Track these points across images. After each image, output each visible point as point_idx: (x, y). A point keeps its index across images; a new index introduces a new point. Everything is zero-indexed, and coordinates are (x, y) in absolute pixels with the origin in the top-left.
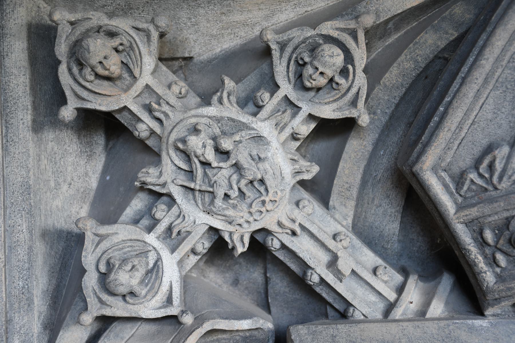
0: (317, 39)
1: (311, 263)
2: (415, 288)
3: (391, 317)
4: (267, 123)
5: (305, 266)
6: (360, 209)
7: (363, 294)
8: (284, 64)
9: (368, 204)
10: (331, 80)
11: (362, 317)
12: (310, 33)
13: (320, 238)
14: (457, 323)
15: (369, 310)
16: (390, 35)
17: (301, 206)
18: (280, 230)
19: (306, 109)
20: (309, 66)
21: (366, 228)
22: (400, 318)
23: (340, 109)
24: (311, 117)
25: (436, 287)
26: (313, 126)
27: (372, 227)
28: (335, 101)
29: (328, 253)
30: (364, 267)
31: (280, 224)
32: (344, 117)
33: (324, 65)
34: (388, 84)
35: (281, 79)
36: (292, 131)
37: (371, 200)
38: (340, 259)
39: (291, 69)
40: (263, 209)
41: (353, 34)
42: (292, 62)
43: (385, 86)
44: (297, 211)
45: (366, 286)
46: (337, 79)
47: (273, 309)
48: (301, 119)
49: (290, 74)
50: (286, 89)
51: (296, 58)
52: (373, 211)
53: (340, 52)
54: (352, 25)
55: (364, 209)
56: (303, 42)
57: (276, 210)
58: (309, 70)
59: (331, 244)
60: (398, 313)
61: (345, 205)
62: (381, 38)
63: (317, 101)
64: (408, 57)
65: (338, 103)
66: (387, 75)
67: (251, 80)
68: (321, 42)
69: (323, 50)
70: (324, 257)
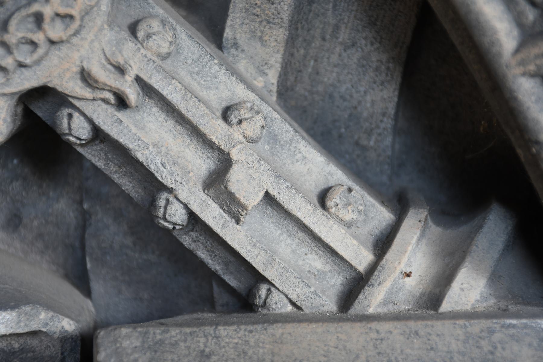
1: (165, 176)
2: (419, 240)
3: (356, 308)
5: (154, 186)
6: (302, 51)
7: (294, 252)
9: (324, 39)
11: (290, 308)
13: (189, 115)
14: (514, 326)
15: (306, 290)
17: (141, 34)
18: (87, 93)
21: (317, 98)
22: (380, 310)
25: (470, 239)
27: (331, 96)
29: (208, 153)
30: (296, 187)
31: (86, 77)
37: (330, 30)
38: (235, 167)
40: (39, 37)
44: (130, 45)
45: (301, 235)
47: (96, 286)
52: (334, 58)
55: (312, 52)
57: (75, 40)
59: (216, 129)
60: (373, 300)
61: (261, 38)
70: (199, 161)
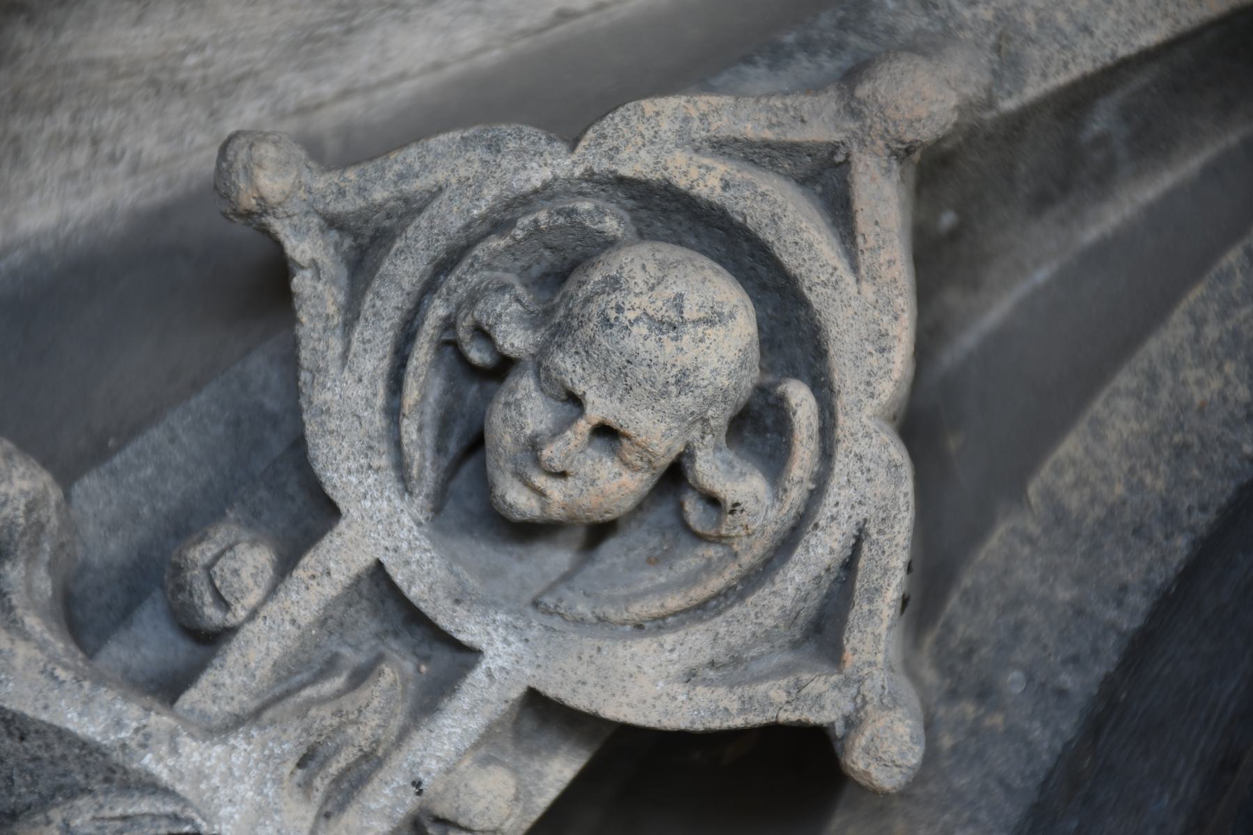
0: (585, 206)
4: (244, 749)
8: (373, 361)
10: (675, 477)
12: (542, 165)
16: (1104, 181)
19: (507, 660)
20: (525, 385)
23: (730, 667)
24: (542, 713)
26: (560, 770)
28: (700, 610)
32: (757, 719)
33: (621, 377)
34: (1074, 502)
35: (347, 460)
36: (410, 802)
39: (411, 394)
41: (826, 180)
42: (422, 354)
43: (1058, 515)
46: (714, 469)
48: (476, 724)
49: (409, 430)
50: (381, 521)
51: (449, 324)
53: (727, 293)
54: (818, 124)
56: (498, 224)
58: (525, 410)
62: (1041, 202)
63: (582, 608)
64: (1212, 332)
65: (719, 624)
66: (1071, 446)
67: (170, 454)
68: (611, 225)
69: (614, 284)
